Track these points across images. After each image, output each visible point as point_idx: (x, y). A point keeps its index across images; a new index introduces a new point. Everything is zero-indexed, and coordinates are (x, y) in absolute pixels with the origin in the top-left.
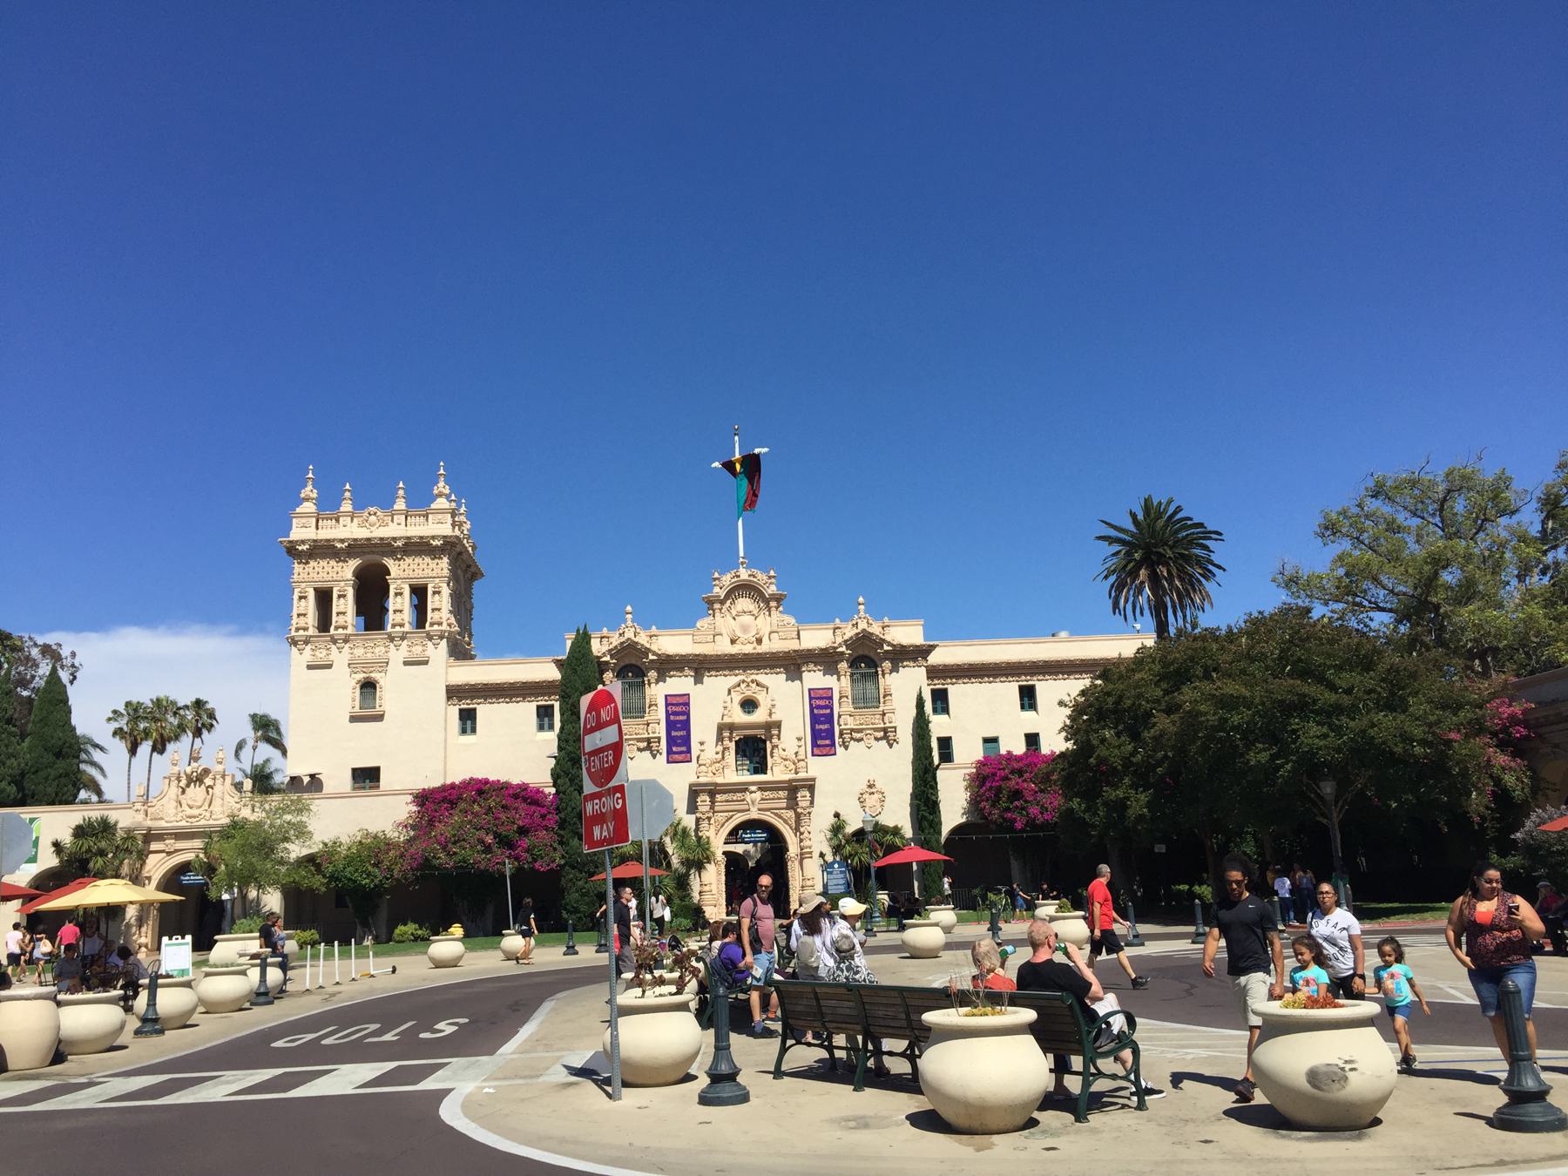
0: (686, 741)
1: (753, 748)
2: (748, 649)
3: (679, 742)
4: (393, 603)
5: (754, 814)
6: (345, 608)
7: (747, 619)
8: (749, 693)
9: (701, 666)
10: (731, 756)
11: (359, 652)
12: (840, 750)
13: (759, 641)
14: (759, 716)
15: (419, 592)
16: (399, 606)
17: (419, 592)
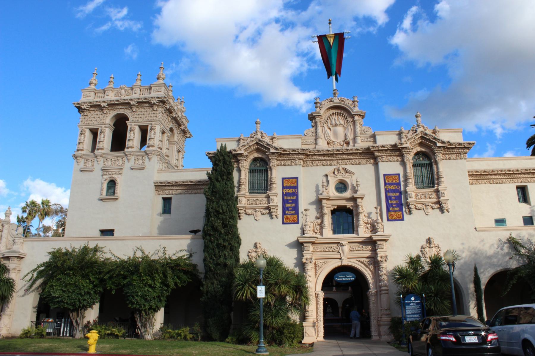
0: (296, 209)
1: (345, 218)
2: (339, 148)
3: (291, 209)
4: (130, 135)
5: (346, 262)
6: (106, 139)
8: (340, 177)
9: (307, 156)
10: (328, 220)
12: (406, 216)
13: (348, 143)
14: (348, 194)
15: (144, 131)
16: (133, 137)
17: (144, 131)
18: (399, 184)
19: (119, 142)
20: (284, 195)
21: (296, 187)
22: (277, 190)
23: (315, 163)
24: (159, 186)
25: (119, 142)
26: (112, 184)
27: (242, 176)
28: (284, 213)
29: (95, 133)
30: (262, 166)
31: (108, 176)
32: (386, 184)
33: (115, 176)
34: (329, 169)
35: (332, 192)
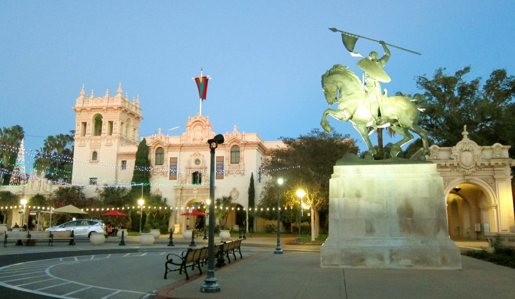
2: (199, 142)
6: (91, 127)
7: (199, 133)
8: (197, 157)
11: (93, 142)
15: (111, 123)
16: (105, 127)
17: (111, 123)
18: (223, 161)
19: (98, 131)
20: (170, 166)
21: (176, 162)
22: (167, 163)
23: (186, 150)
24: (119, 155)
25: (98, 131)
26: (95, 154)
27: (152, 157)
28: (170, 175)
29: (85, 124)
30: (160, 152)
31: (93, 150)
32: (217, 161)
33: (97, 150)
34: (193, 153)
35: (193, 165)
